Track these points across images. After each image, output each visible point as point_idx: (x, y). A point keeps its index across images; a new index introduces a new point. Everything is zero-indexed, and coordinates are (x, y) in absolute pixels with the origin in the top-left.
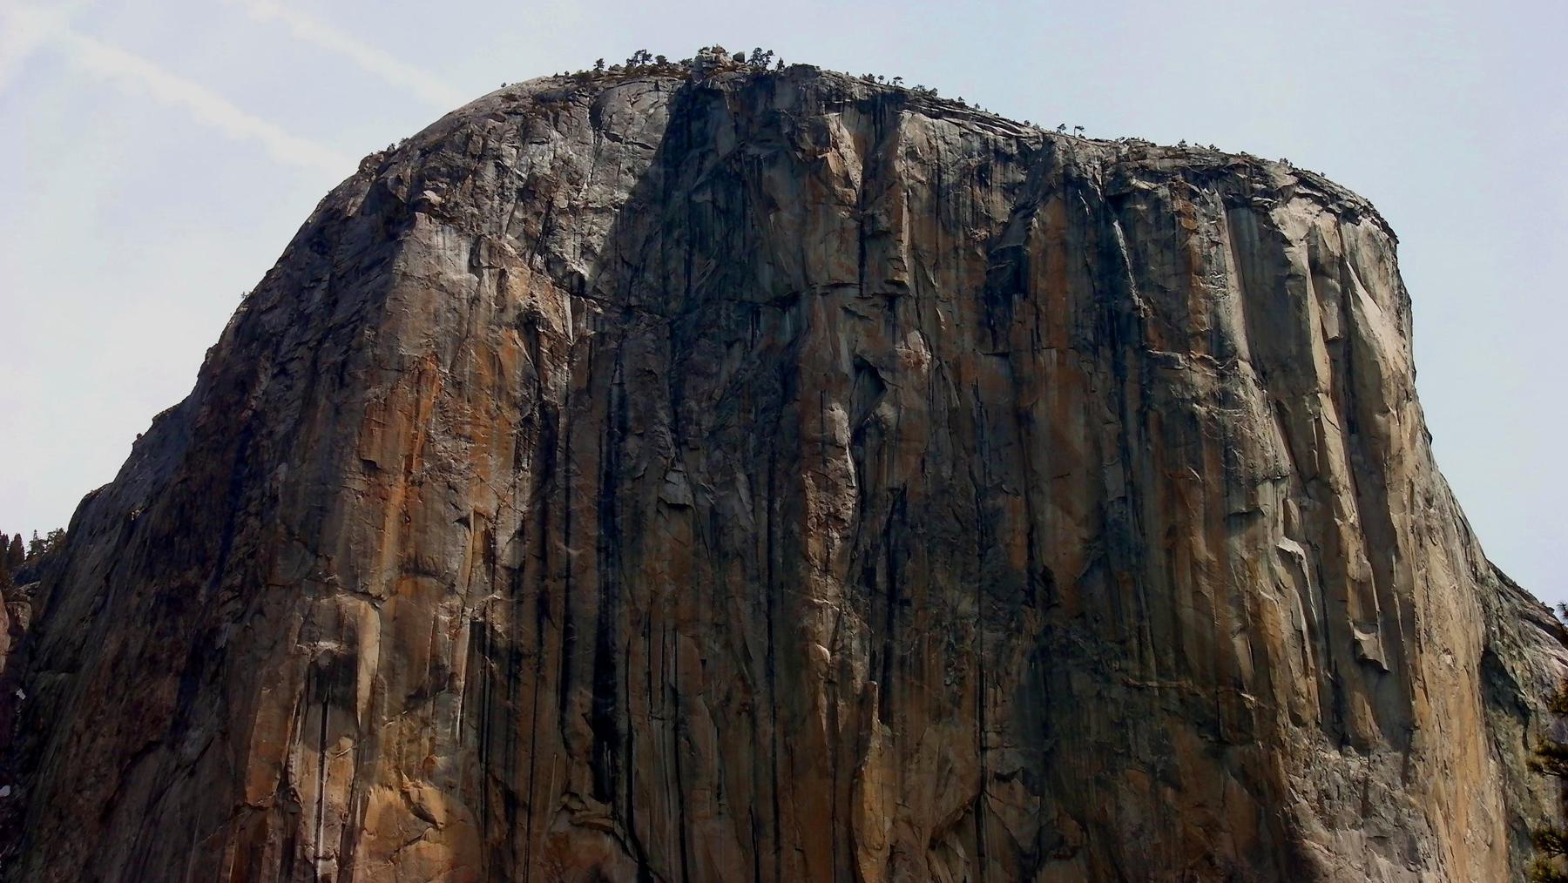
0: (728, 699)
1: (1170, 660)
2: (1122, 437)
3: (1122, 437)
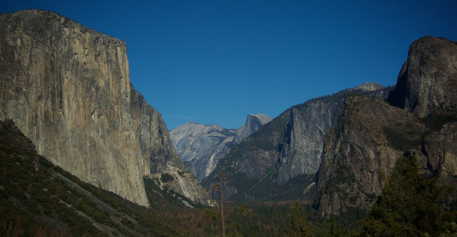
0: (73, 99)
1: (112, 97)
2: (108, 73)
3: (108, 73)
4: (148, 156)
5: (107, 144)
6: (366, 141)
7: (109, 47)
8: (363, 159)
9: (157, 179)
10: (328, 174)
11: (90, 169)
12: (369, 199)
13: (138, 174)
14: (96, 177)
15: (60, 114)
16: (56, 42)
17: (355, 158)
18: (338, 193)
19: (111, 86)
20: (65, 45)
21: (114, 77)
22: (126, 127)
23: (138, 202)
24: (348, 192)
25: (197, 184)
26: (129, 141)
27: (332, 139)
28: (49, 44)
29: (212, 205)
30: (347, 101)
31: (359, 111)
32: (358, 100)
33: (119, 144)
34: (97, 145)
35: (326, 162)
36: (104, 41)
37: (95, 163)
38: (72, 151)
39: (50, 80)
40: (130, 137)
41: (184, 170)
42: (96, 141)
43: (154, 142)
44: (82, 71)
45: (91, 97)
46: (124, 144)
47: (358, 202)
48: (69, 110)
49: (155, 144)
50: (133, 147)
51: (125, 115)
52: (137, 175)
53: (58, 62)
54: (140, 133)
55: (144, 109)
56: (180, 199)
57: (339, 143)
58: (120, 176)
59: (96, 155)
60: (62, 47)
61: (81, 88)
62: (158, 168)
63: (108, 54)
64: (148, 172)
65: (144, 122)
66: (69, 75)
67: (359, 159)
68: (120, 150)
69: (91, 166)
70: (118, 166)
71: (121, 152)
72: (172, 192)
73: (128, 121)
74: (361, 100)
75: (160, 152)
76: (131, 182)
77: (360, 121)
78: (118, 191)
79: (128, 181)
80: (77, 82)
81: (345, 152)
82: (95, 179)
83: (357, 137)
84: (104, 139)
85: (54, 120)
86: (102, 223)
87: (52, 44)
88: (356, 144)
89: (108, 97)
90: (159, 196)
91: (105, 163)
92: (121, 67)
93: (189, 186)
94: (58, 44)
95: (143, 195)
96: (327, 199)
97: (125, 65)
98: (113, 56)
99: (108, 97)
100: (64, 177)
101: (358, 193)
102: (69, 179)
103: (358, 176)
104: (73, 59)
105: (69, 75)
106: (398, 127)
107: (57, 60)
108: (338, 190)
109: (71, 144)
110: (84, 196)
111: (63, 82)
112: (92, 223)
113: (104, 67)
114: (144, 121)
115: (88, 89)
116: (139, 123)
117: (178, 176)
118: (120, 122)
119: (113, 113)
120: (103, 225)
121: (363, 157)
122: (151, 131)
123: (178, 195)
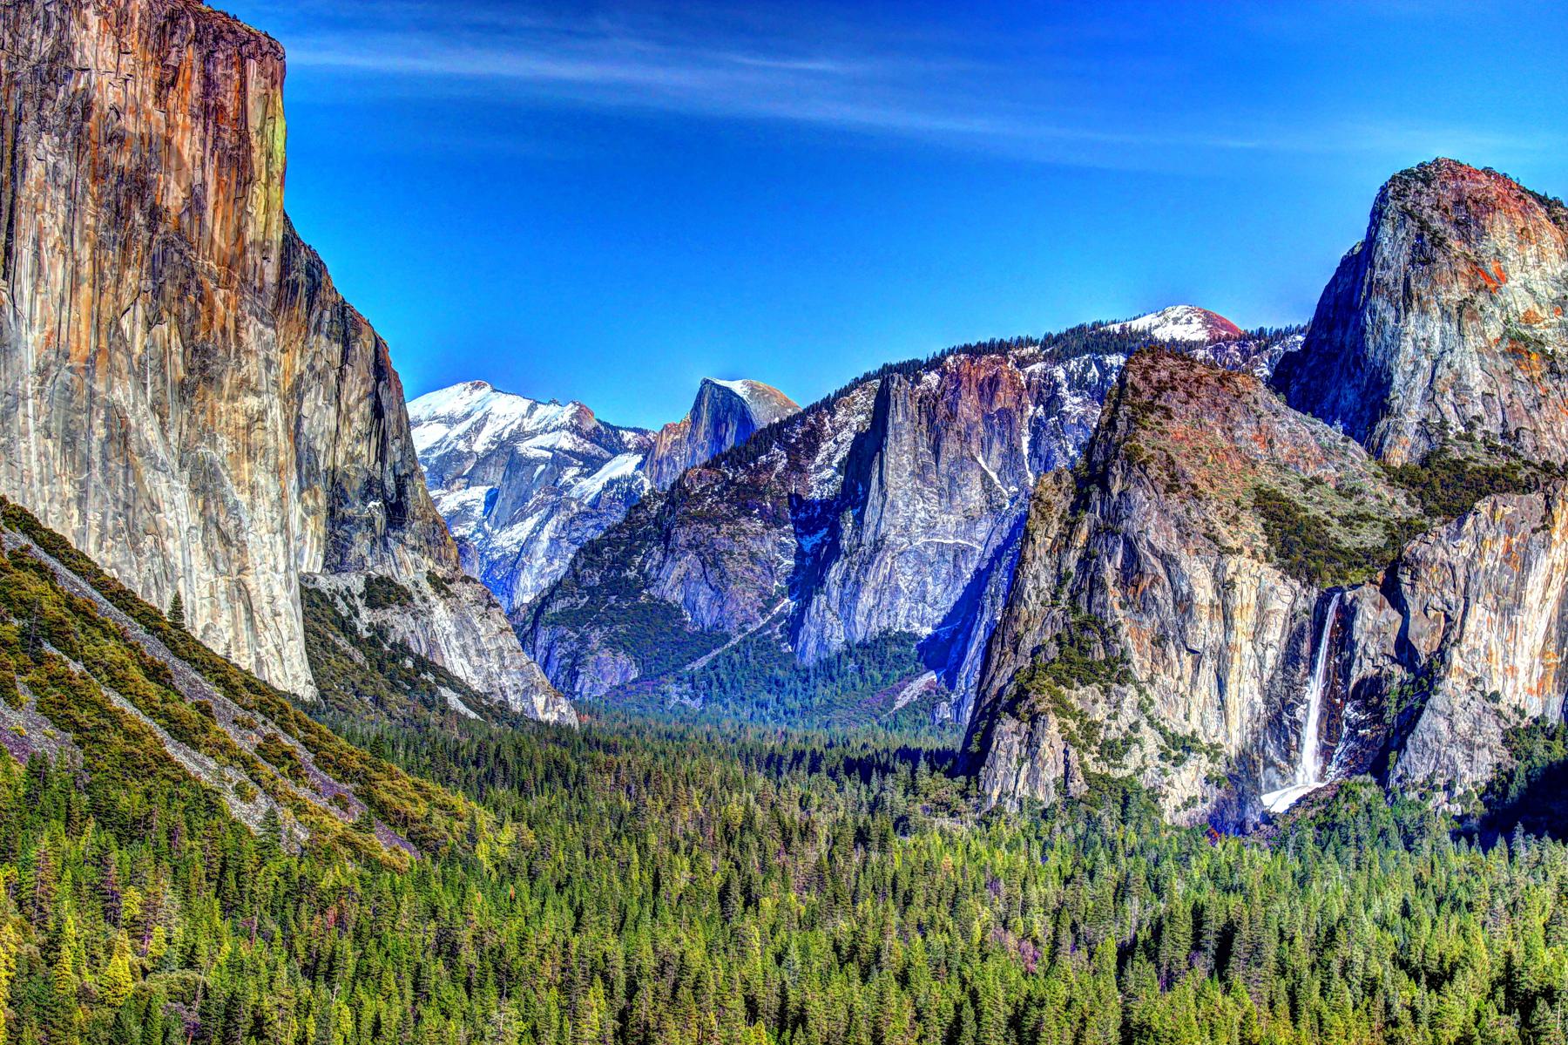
0: (55, 246)
1: (207, 254)
2: (203, 159)
3: (203, 159)
4: (321, 501)
5: (173, 436)
6: (1188, 535)
7: (216, 55)
8: (1170, 601)
9: (345, 593)
10: (1027, 644)
11: (98, 526)
12: (1174, 753)
13: (282, 567)
14: (118, 560)
17: (1139, 594)
18: (1063, 720)
20: (47, 29)
21: (225, 178)
22: (253, 379)
23: (272, 676)
24: (1098, 719)
25: (502, 631)
26: (257, 436)
27: (1060, 512)
29: (552, 717)
30: (1131, 374)
31: (1170, 418)
32: (1172, 375)
33: (219, 442)
34: (133, 436)
35: (1025, 596)
36: (198, 31)
38: (33, 449)
40: (263, 421)
42: (133, 422)
43: (350, 449)
44: (102, 140)
45: (125, 247)
46: (240, 444)
47: (1132, 760)
48: (35, 286)
49: (352, 458)
50: (271, 462)
51: (251, 330)
53: (12, 91)
54: (300, 408)
55: (321, 315)
56: (430, 678)
57: (1085, 530)
58: (211, 568)
59: (126, 474)
60: (34, 37)
61: (91, 205)
62: (354, 552)
63: (208, 83)
65: (318, 368)
66: (50, 149)
67: (1154, 598)
69: (104, 515)
70: (205, 529)
71: (224, 473)
72: (403, 649)
73: (262, 354)
74: (1182, 374)
75: (370, 491)
76: (253, 594)
77: (1173, 455)
78: (200, 626)
79: (241, 591)
81: (1104, 566)
82: (114, 571)
83: (1156, 514)
84: (161, 417)
86: (195, 746)
88: (1148, 542)
89: (194, 253)
90: (351, 659)
92: (255, 140)
95: (296, 650)
96: (1017, 739)
98: (229, 95)
100: (42, 554)
101: (1135, 727)
102: (62, 562)
103: (1140, 665)
104: (72, 90)
105: (50, 149)
106: (1308, 494)
107: (10, 85)
108: (1063, 709)
109: (31, 421)
110: (121, 636)
111: (24, 176)
112: (161, 744)
115: (119, 216)
116: (297, 367)
117: (427, 589)
118: (232, 355)
119: (204, 318)
120: (199, 756)
121: (1171, 594)
122: (343, 407)
123: (423, 664)
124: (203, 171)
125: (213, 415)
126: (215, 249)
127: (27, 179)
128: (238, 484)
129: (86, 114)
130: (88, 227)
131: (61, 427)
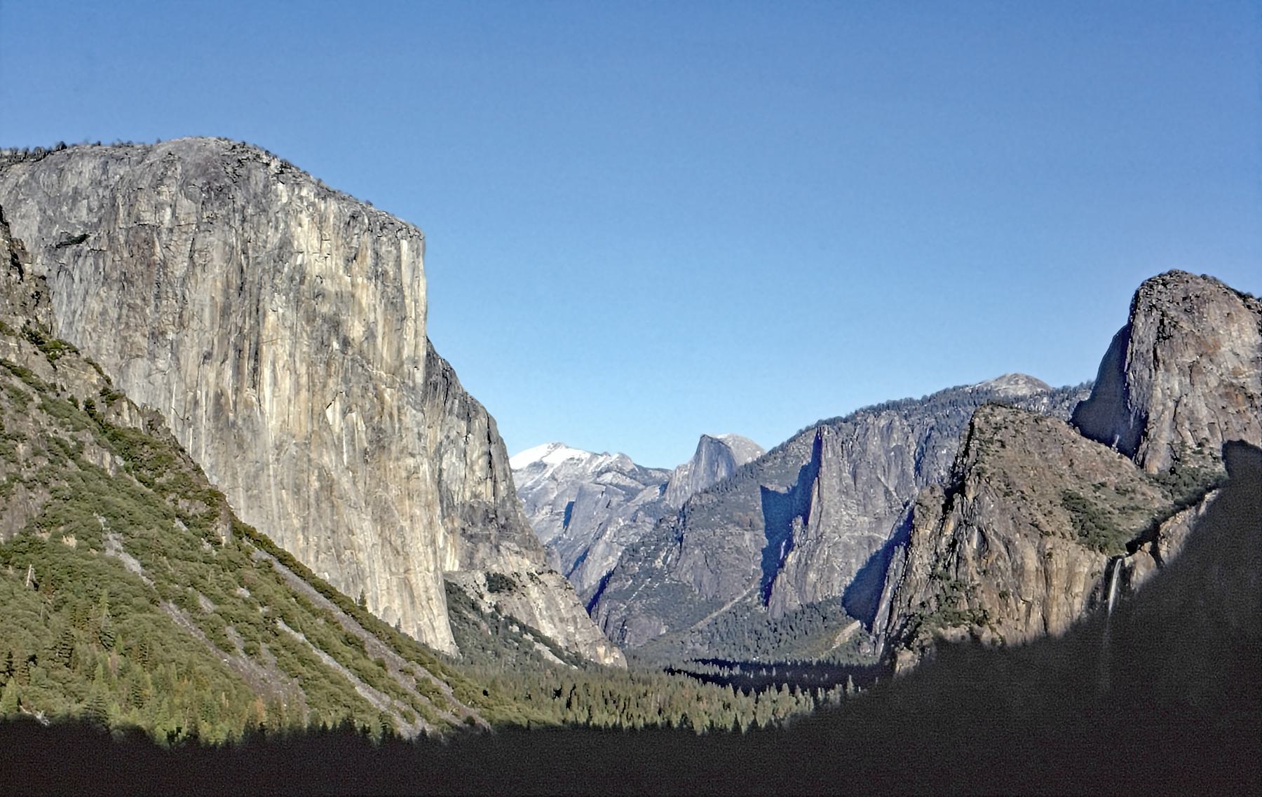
0: (284, 366)
2: (374, 306)
3: (374, 306)
5: (361, 486)
8: (1010, 569)
13: (432, 568)
14: (328, 567)
15: (251, 402)
16: (255, 219)
19: (379, 339)
20: (276, 228)
22: (410, 446)
28: (238, 223)
34: (335, 487)
35: (914, 569)
36: (370, 224)
37: (329, 532)
38: (274, 496)
39: (234, 315)
41: (544, 565)
45: (328, 364)
48: (273, 392)
50: (423, 499)
52: (429, 571)
54: (441, 464)
59: (332, 511)
61: (306, 338)
63: (377, 255)
64: (454, 565)
65: (452, 438)
67: (999, 568)
68: (390, 503)
70: (383, 545)
71: (394, 508)
72: (511, 620)
73: (416, 430)
74: (1011, 418)
76: (414, 586)
79: (406, 585)
80: (299, 324)
82: (326, 574)
83: (998, 511)
85: (236, 416)
87: (246, 224)
88: (993, 530)
89: (370, 366)
91: (353, 535)
92: (407, 292)
93: (553, 608)
94: (259, 224)
97: (416, 287)
99: (370, 366)
106: (1098, 494)
109: (272, 479)
111: (264, 322)
113: (365, 290)
114: (453, 434)
115: (324, 345)
118: (396, 431)
122: (468, 460)
124: (375, 313)
125: (385, 470)
126: (384, 362)
127: (266, 324)
128: (403, 515)
129: (302, 282)
130: (304, 353)
131: (291, 483)
